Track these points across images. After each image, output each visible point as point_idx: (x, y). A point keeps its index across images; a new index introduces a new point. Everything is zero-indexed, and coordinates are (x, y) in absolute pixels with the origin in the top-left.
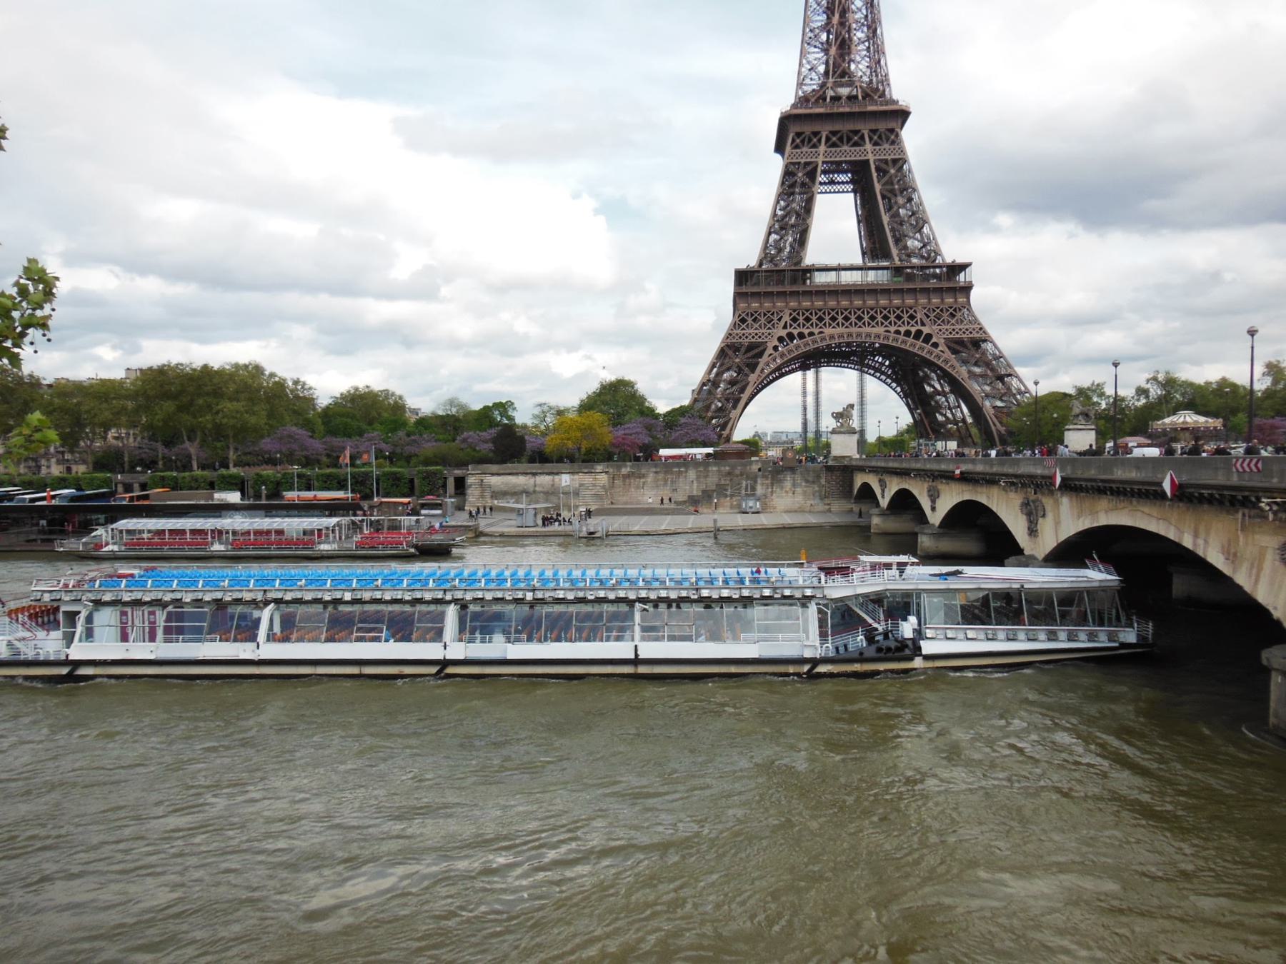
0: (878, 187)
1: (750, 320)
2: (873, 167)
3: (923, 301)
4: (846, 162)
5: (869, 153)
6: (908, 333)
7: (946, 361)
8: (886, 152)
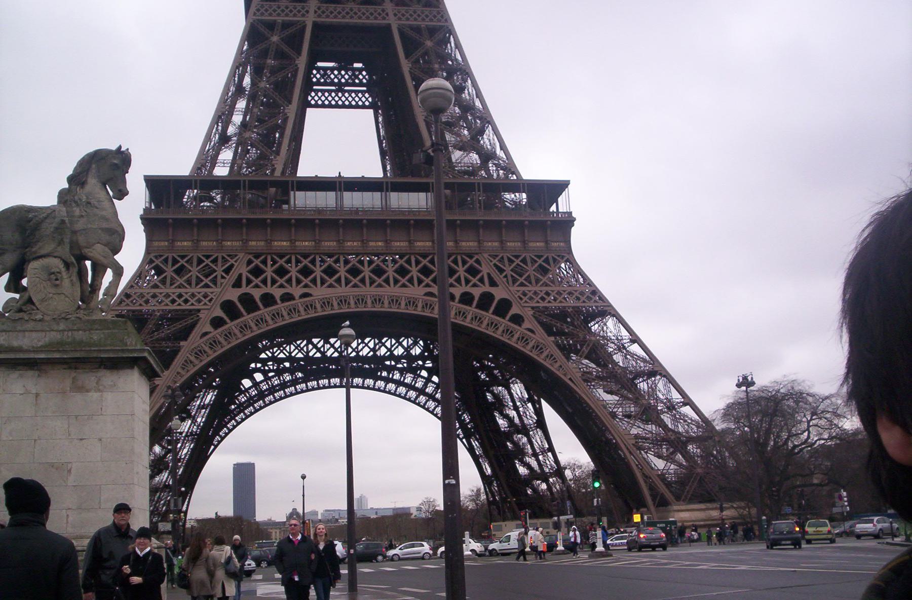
3: (493, 245)
6: (467, 299)
7: (538, 347)
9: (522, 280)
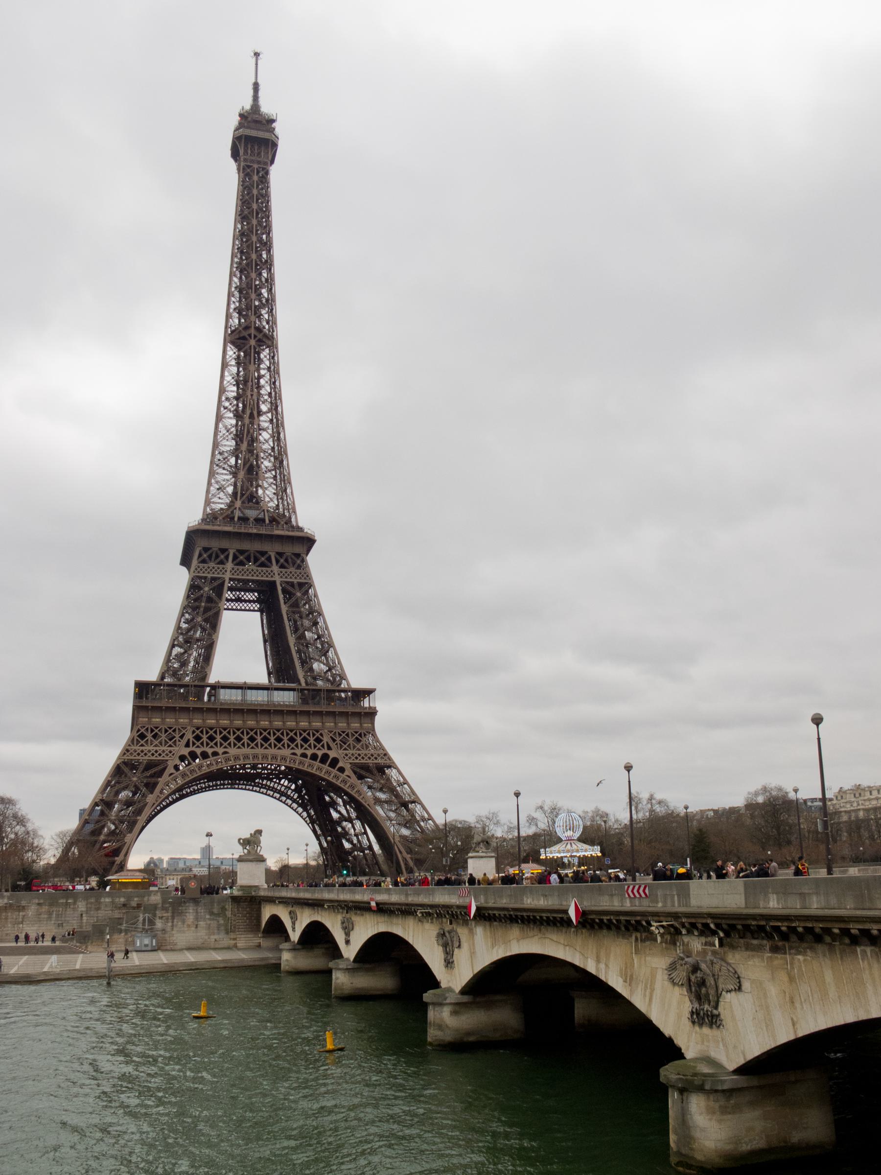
0: (284, 609)
1: (149, 736)
2: (279, 588)
3: (330, 724)
4: (253, 581)
5: (276, 575)
9: (345, 746)
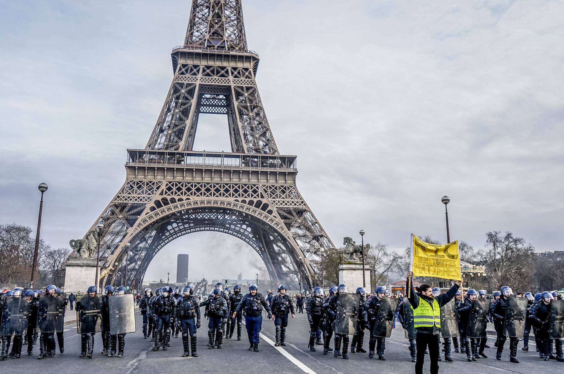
1: (135, 187)
5: (231, 81)
7: (277, 224)
8: (243, 82)
9: (274, 196)
